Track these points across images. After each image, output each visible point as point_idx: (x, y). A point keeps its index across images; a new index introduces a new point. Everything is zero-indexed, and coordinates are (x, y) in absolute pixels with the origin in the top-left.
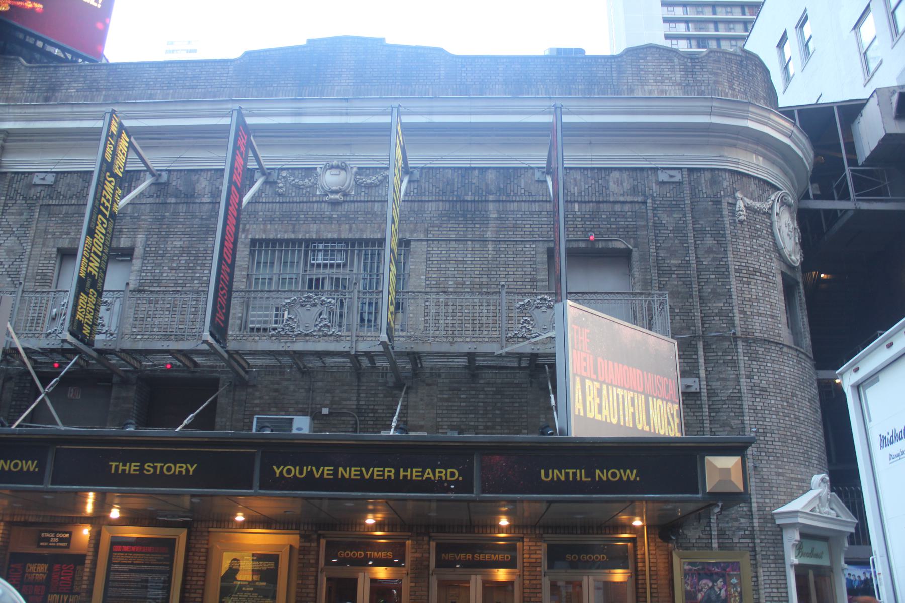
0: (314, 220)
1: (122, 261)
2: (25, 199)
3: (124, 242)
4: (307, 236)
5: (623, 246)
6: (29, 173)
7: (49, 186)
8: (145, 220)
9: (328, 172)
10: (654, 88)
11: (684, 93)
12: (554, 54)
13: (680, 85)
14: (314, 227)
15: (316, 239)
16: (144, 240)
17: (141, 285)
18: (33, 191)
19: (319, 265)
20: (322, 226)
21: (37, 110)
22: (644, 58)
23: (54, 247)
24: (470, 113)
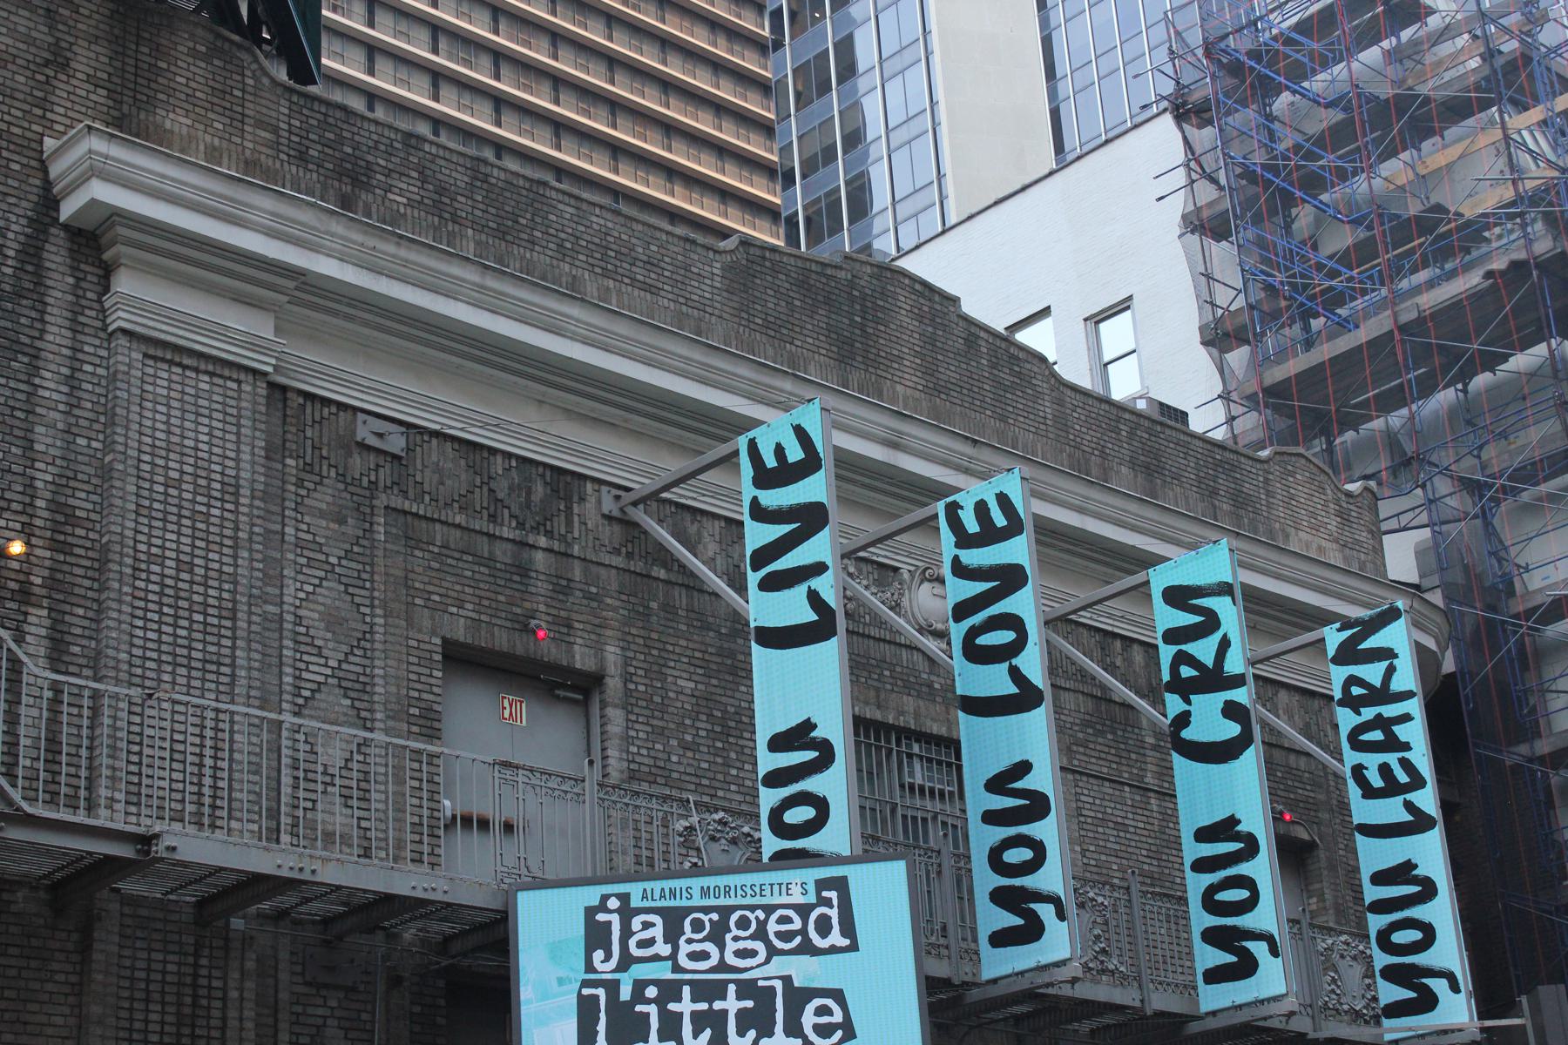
0: (908, 688)
1: (566, 699)
2: (341, 477)
3: (582, 659)
4: (901, 722)
5: (1305, 836)
6: (340, 405)
7: (395, 457)
8: (615, 609)
9: (926, 585)
10: (1309, 537)
11: (1345, 559)
12: (1156, 416)
13: (1336, 541)
14: (909, 703)
15: (914, 732)
16: (620, 661)
17: (633, 776)
18: (357, 462)
19: (922, 789)
20: (921, 703)
21: (403, 253)
22: (1292, 474)
23: (434, 633)
24: (1134, 529)
